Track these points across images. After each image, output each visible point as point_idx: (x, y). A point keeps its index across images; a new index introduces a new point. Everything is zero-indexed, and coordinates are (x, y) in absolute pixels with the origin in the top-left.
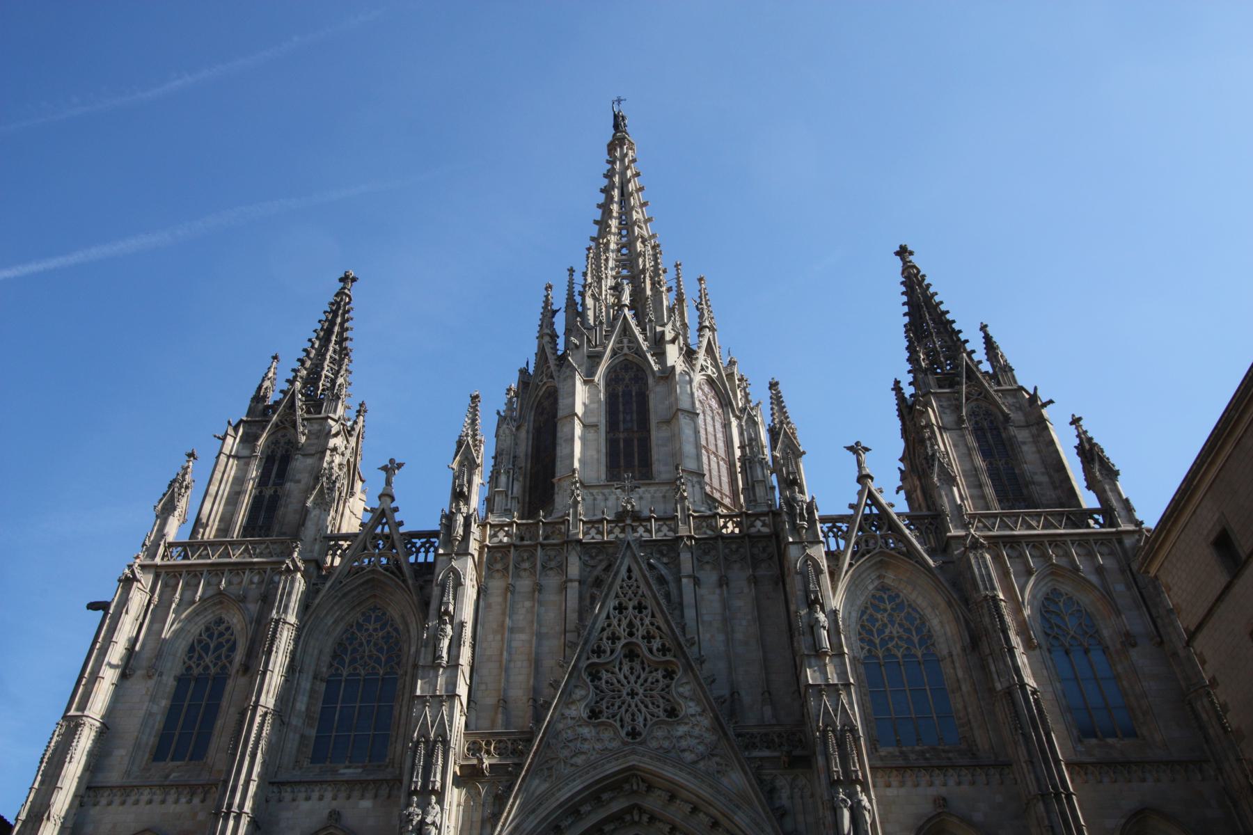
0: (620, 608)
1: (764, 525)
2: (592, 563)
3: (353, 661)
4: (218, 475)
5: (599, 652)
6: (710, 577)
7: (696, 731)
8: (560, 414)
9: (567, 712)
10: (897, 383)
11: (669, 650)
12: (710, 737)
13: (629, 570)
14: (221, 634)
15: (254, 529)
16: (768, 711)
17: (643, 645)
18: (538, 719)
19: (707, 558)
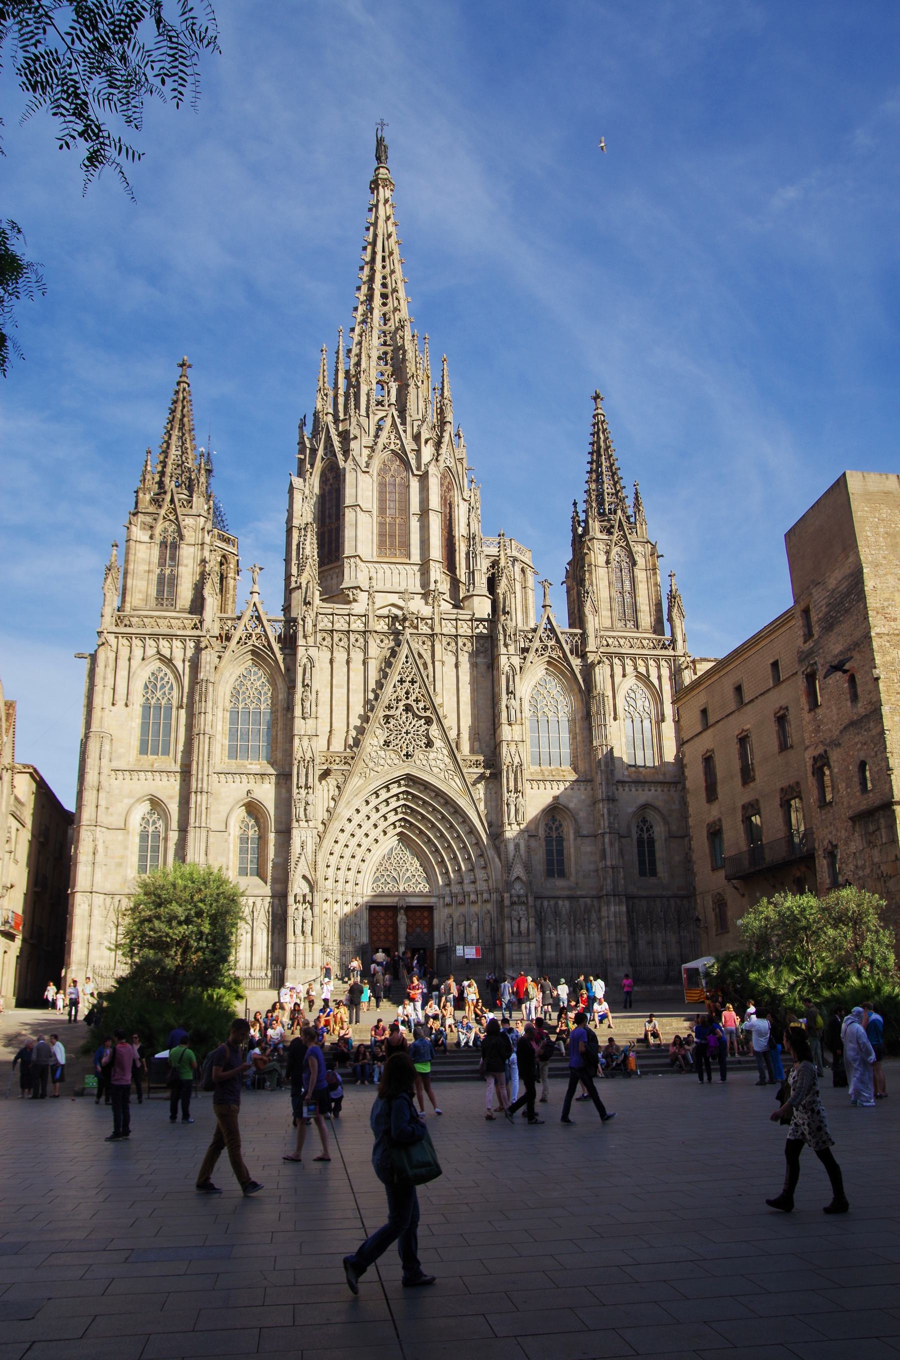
0: (401, 681)
1: (484, 627)
2: (382, 645)
3: (244, 699)
4: (131, 557)
5: (389, 707)
6: (450, 659)
7: (440, 756)
8: (348, 501)
9: (372, 742)
10: (575, 504)
11: (428, 709)
12: (447, 760)
13: (407, 657)
14: (162, 679)
15: (162, 599)
16: (477, 745)
17: (414, 704)
18: (357, 743)
19: (449, 648)
